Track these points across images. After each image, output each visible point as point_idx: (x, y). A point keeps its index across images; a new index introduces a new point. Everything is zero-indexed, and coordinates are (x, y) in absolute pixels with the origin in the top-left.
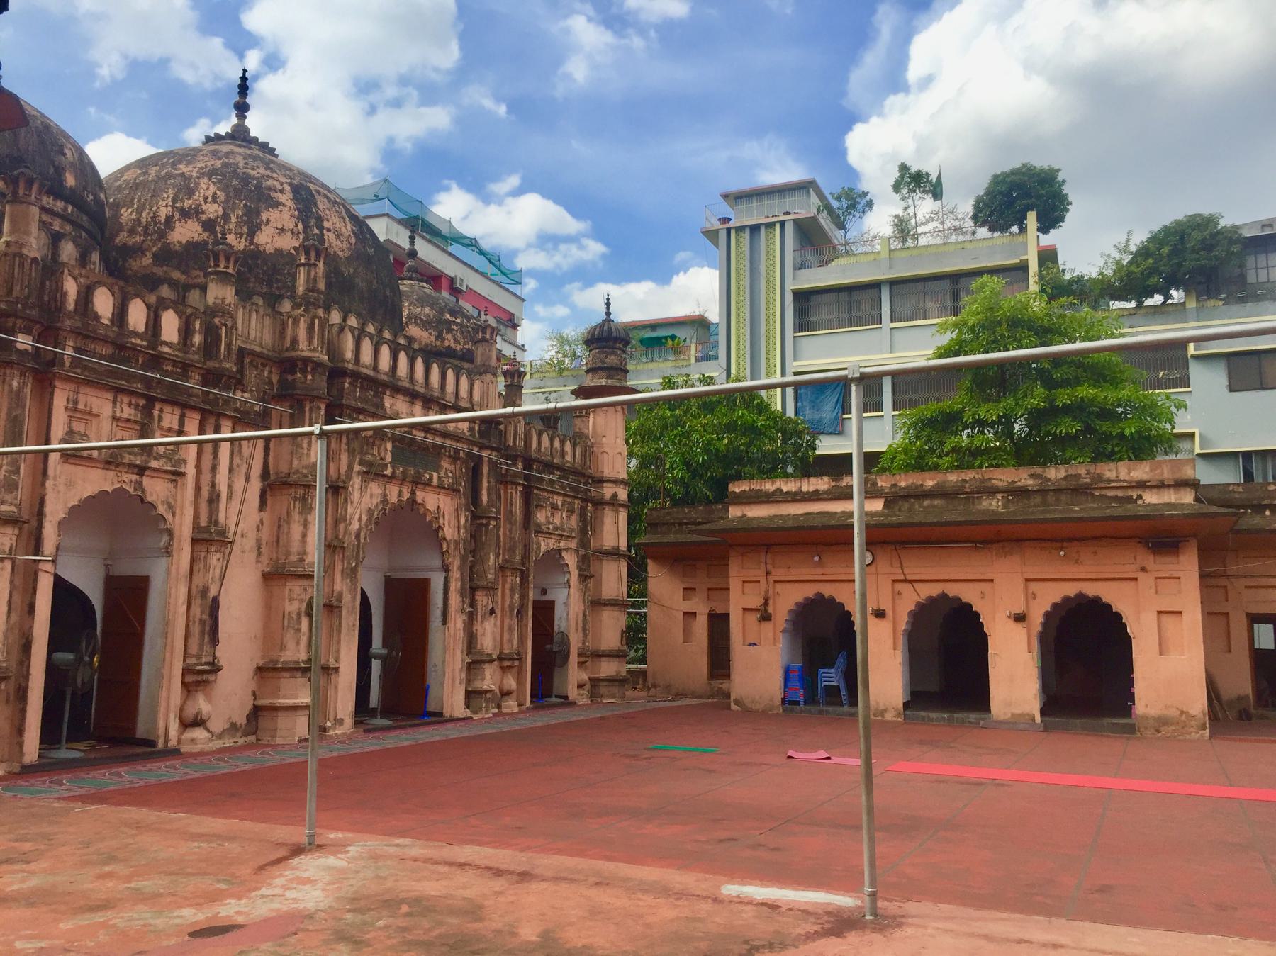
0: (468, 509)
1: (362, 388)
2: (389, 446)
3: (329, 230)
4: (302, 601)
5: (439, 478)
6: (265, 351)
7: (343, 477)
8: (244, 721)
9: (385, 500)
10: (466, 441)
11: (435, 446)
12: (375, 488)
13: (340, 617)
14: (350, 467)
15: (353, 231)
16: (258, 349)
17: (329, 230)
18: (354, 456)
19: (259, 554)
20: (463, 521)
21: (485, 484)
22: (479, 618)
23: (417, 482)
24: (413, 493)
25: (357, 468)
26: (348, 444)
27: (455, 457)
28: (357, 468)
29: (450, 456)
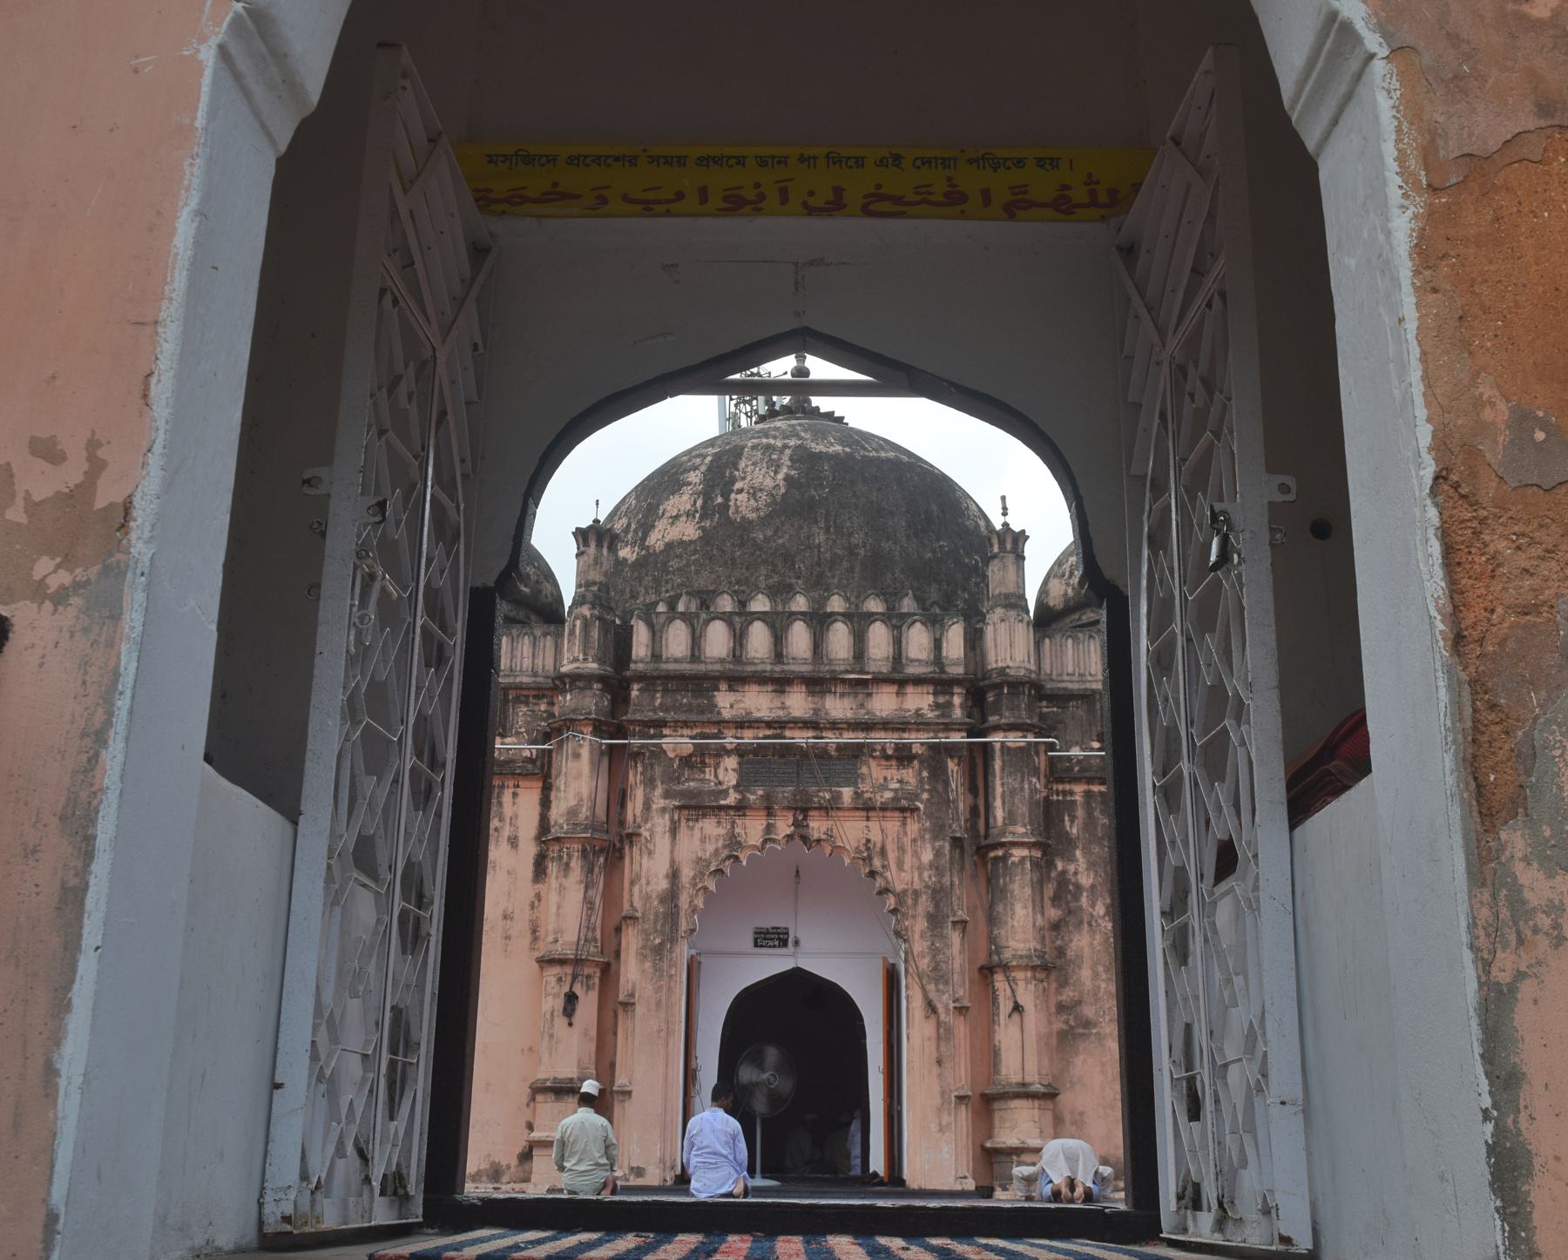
0: (935, 838)
1: (665, 691)
2: (731, 762)
3: (740, 491)
4: (556, 996)
5: (857, 795)
6: (540, 679)
7: (639, 820)
8: (514, 1162)
9: (734, 842)
10: (921, 725)
11: (840, 748)
12: (712, 828)
13: (633, 1017)
14: (647, 805)
15: (787, 478)
16: (526, 680)
17: (740, 491)
18: (654, 788)
19: (535, 939)
20: (927, 856)
21: (999, 790)
22: (1002, 1021)
23: (802, 809)
24: (796, 824)
25: (659, 802)
26: (645, 769)
27: (903, 756)
28: (659, 802)
29: (888, 758)
